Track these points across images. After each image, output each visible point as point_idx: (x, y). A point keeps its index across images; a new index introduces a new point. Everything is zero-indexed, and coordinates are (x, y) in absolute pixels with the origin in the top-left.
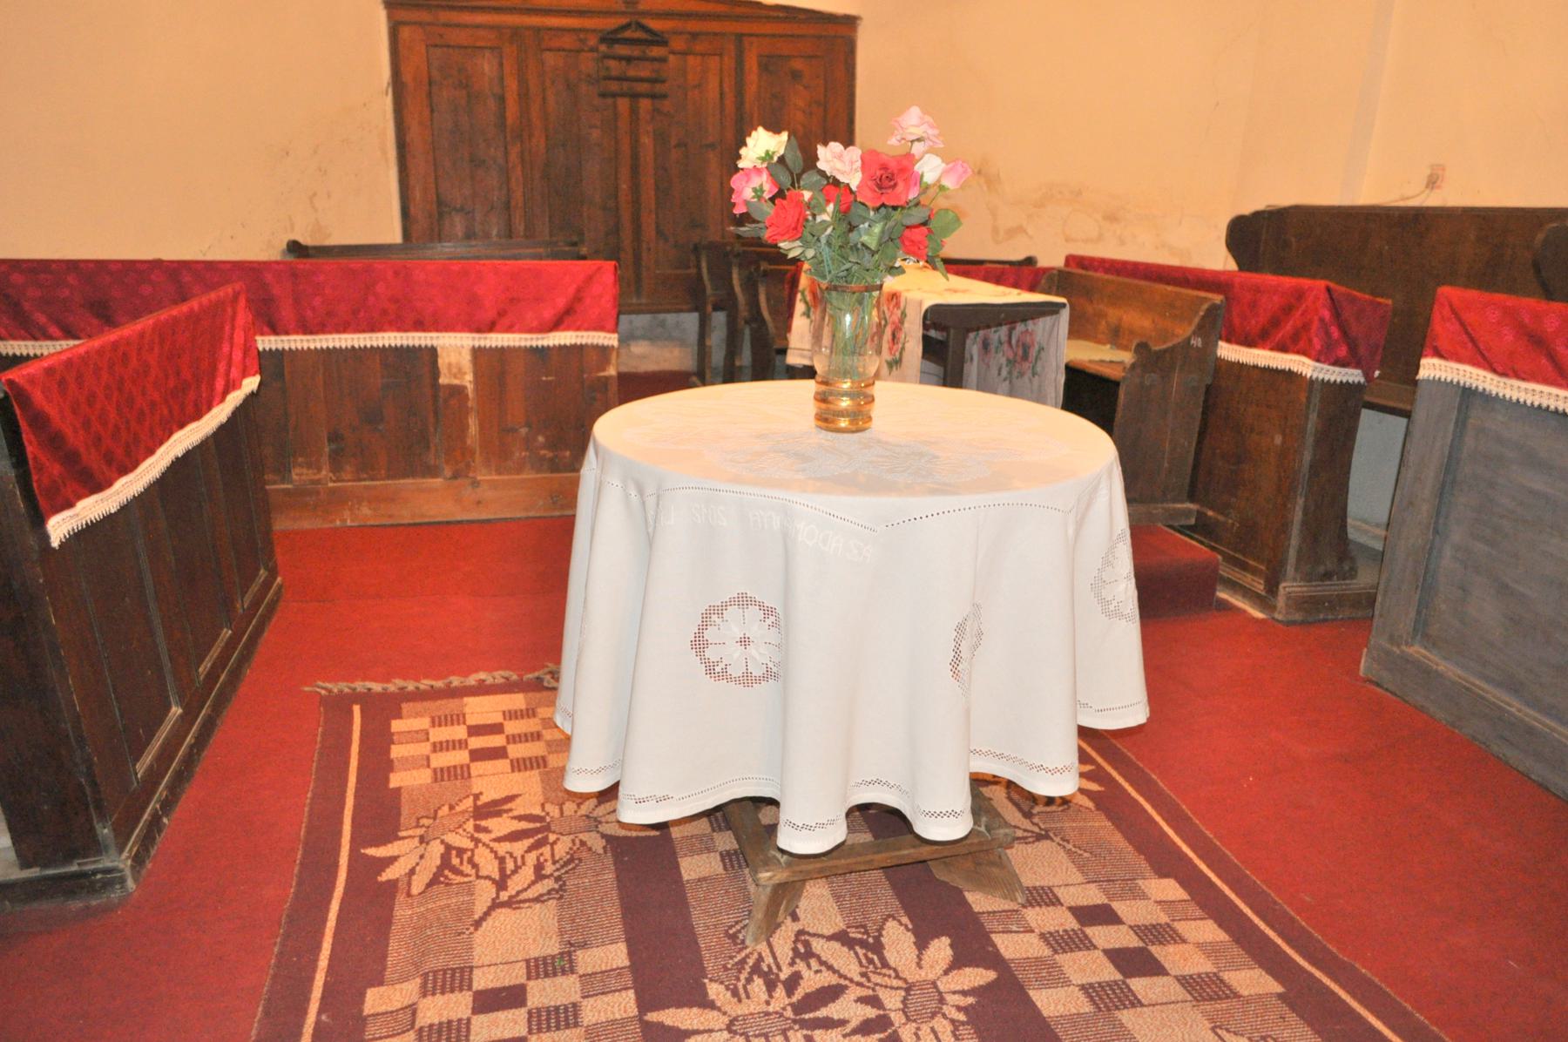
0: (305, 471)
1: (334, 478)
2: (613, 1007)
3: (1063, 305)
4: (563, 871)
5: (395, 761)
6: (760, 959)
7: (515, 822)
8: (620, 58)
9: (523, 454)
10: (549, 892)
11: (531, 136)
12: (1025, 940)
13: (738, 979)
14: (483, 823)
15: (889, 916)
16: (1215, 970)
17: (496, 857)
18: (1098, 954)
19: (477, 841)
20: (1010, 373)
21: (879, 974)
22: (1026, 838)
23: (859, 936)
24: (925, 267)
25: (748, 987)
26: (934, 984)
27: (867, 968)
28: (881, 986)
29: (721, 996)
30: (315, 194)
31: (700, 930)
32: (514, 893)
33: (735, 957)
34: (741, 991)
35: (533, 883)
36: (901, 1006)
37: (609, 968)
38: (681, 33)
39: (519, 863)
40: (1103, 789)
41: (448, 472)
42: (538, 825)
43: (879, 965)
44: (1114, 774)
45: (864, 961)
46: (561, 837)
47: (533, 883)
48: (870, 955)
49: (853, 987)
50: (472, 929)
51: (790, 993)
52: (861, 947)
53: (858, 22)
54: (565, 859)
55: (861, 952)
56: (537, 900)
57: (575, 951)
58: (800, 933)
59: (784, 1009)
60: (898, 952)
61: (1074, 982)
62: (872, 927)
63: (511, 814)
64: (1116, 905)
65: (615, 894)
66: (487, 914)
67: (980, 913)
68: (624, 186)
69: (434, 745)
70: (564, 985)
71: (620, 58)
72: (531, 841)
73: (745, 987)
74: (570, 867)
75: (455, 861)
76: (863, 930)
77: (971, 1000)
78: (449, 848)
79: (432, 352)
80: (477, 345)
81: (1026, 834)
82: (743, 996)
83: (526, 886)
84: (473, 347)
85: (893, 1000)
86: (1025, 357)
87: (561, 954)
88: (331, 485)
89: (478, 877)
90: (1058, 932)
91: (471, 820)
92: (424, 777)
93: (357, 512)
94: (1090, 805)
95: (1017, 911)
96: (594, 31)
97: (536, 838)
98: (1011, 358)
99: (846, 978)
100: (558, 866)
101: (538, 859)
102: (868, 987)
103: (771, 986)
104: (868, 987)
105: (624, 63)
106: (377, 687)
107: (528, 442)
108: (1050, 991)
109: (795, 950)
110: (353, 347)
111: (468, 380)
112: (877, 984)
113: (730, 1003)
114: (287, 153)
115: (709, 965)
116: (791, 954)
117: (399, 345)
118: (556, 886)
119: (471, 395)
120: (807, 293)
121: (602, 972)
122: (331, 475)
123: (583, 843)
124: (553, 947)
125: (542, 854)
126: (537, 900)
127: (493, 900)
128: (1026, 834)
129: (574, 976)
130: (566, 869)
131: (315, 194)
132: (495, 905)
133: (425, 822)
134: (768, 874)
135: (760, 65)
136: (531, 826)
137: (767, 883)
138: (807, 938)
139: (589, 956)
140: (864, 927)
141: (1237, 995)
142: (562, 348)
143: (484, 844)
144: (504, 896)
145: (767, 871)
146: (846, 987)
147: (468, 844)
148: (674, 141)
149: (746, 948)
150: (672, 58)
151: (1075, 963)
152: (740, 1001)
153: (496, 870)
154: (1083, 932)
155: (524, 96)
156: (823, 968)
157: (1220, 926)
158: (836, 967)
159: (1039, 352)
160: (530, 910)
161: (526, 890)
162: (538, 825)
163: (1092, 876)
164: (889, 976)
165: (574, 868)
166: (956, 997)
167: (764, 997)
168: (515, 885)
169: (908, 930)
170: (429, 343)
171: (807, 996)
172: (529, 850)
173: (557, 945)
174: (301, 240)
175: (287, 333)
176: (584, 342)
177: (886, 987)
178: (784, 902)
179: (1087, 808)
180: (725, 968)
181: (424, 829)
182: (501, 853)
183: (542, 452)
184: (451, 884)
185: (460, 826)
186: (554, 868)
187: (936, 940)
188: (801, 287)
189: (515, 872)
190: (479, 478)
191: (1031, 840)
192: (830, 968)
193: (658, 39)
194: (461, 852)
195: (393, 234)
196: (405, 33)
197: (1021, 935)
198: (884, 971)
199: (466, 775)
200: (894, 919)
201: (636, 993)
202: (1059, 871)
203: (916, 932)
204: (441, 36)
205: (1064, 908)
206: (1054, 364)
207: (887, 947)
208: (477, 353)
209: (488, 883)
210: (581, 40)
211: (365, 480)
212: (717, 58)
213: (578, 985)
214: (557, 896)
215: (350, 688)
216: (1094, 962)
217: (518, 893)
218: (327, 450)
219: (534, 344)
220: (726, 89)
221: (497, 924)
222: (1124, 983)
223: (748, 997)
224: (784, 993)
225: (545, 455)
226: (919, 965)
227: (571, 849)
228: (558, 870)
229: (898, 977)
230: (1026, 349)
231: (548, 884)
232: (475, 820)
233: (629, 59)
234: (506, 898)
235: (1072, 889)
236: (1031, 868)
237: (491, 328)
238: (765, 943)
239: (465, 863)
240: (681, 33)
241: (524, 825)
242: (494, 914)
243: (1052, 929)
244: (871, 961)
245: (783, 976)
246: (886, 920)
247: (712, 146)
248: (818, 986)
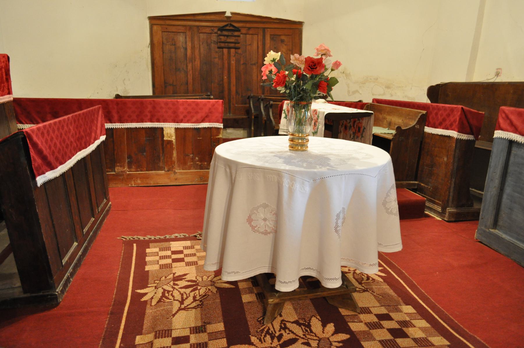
0: (119, 168)
1: (129, 171)
2: (219, 344)
3: (372, 113)
4: (203, 299)
5: (147, 262)
6: (269, 329)
7: (187, 282)
8: (224, 36)
9: (191, 163)
10: (198, 305)
11: (195, 61)
12: (359, 325)
13: (261, 336)
14: (176, 282)
15: (313, 316)
16: (426, 337)
17: (180, 294)
18: (385, 330)
19: (174, 288)
20: (354, 137)
21: (310, 335)
22: (360, 291)
23: (303, 322)
24: (325, 102)
25: (265, 338)
26: (328, 339)
27: (305, 333)
28: (310, 339)
29: (256, 341)
30: (125, 79)
31: (248, 319)
32: (186, 305)
33: (260, 328)
34: (262, 339)
35: (193, 302)
36: (317, 346)
37: (218, 331)
38: (245, 27)
39: (188, 296)
40: (386, 275)
41: (166, 169)
42: (194, 283)
43: (309, 332)
44: (390, 270)
45: (304, 330)
46: (202, 288)
47: (193, 302)
48: (306, 328)
49: (300, 339)
50: (172, 317)
51: (279, 341)
52: (303, 326)
53: (303, 24)
54: (203, 295)
55: (303, 327)
56: (194, 308)
57: (206, 325)
58: (283, 320)
59: (277, 346)
60: (316, 328)
61: (377, 339)
62: (307, 319)
63: (185, 280)
64: (391, 314)
65: (220, 306)
66: (177, 312)
67: (344, 315)
68: (225, 77)
69: (160, 257)
70: (202, 336)
71: (224, 36)
72: (192, 288)
73: (264, 338)
74: (205, 297)
75: (167, 295)
76: (304, 320)
77: (341, 344)
78: (164, 290)
79: (162, 129)
80: (176, 127)
81: (360, 290)
82: (263, 341)
83: (190, 303)
84: (175, 128)
85: (314, 344)
86: (359, 131)
87: (202, 326)
88: (128, 173)
89: (174, 300)
90: (371, 322)
91: (172, 281)
92: (156, 267)
93: (136, 181)
94: (382, 280)
95: (357, 315)
97: (194, 288)
98: (354, 131)
99: (298, 336)
100: (201, 297)
101: (194, 294)
102: (306, 339)
103: (272, 338)
104: (306, 339)
105: (226, 37)
106: (142, 238)
107: (193, 159)
108: (368, 342)
109: (281, 326)
110: (136, 127)
111: (173, 139)
112: (309, 338)
113: (258, 343)
114: (116, 66)
115: (252, 331)
116: (279, 328)
117: (151, 127)
118: (200, 303)
119: (174, 144)
120: (286, 111)
121: (215, 332)
122: (128, 169)
123: (209, 290)
124: (199, 324)
125: (195, 293)
126: (194, 308)
127: (179, 307)
128: (360, 290)
129: (206, 333)
130: (203, 298)
131: (125, 79)
132: (180, 309)
133: (157, 282)
134: (272, 300)
136: (192, 284)
137: (272, 303)
138: (285, 322)
139: (211, 327)
140: (304, 319)
141: (433, 345)
142: (204, 128)
143: (176, 289)
144: (183, 306)
145: (272, 299)
146: (298, 339)
147: (171, 289)
148: (242, 62)
149: (264, 325)
150: (241, 35)
151: (377, 333)
152: (262, 343)
153: (180, 298)
154: (380, 323)
155: (193, 48)
156: (290, 333)
157: (427, 322)
158: (295, 332)
159: (364, 129)
160: (191, 311)
161: (190, 304)
162: (194, 283)
163: (382, 304)
164: (313, 336)
165: (206, 298)
166: (336, 343)
167: (270, 341)
168: (186, 303)
169: (319, 320)
170: (161, 126)
171: (285, 342)
172: (191, 291)
173: (200, 323)
174: (120, 94)
175: (115, 123)
176: (212, 127)
177: (312, 339)
178: (277, 310)
179: (381, 282)
180: (257, 332)
181: (156, 284)
182: (182, 292)
183: (197, 163)
184: (165, 302)
185: (168, 283)
186: (199, 297)
187: (329, 324)
188: (284, 109)
189: (186, 299)
190: (176, 171)
191: (362, 291)
192: (293, 332)
193: (238, 30)
194: (168, 292)
195: (149, 92)
196: (155, 27)
197: (358, 323)
198: (311, 334)
199: (170, 267)
200: (315, 317)
201: (227, 340)
202: (371, 302)
203: (322, 321)
204: (166, 28)
205: (373, 315)
206: (369, 133)
207: (312, 326)
208: (177, 129)
209: (177, 302)
210: (212, 30)
211: (139, 171)
212: (257, 36)
213: (207, 336)
214: (200, 307)
215: (133, 238)
216: (384, 333)
217: (188, 305)
218: (127, 161)
219: (195, 127)
221: (180, 315)
222: (394, 340)
223: (265, 342)
224: (277, 341)
225: (198, 164)
226: (323, 332)
227: (205, 291)
228: (201, 298)
229: (316, 336)
230: (359, 128)
231: (198, 303)
232: (173, 282)
233: (227, 36)
234: (183, 307)
235: (376, 308)
236: (362, 301)
237: (181, 121)
238: (270, 324)
239: (170, 295)
240: (245, 27)
241: (190, 283)
242: (179, 312)
243: (369, 321)
244: (307, 331)
245: (277, 335)
246: (312, 317)
247: (255, 64)
248: (289, 338)
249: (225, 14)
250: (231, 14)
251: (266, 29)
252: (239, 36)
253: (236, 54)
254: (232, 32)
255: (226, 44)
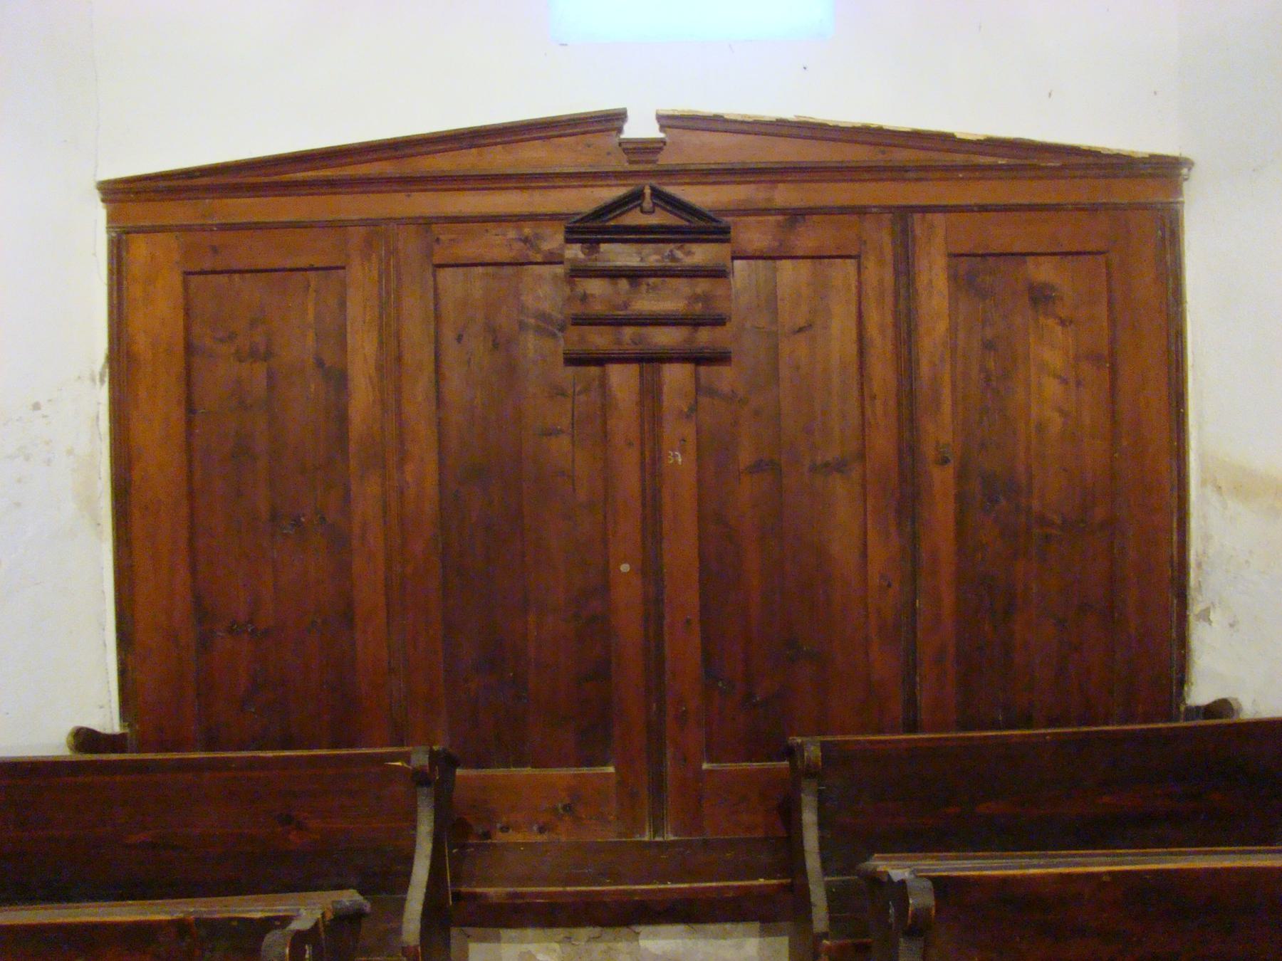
8: (613, 274)
38: (766, 211)
53: (1185, 171)
68: (625, 568)
96: (554, 217)
105: (624, 284)
135: (953, 277)
148: (745, 456)
150: (738, 264)
196: (140, 248)
204: (215, 250)
210: (526, 240)
212: (850, 265)
220: (873, 331)
233: (635, 275)
240: (766, 211)
247: (840, 467)
249: (620, 130)
250: (663, 128)
251: (917, 216)
252: (718, 273)
253: (704, 400)
254: (667, 248)
255: (628, 332)
